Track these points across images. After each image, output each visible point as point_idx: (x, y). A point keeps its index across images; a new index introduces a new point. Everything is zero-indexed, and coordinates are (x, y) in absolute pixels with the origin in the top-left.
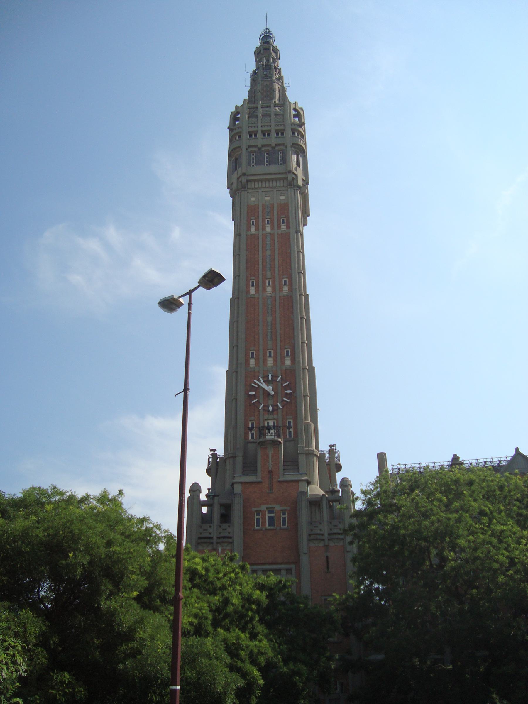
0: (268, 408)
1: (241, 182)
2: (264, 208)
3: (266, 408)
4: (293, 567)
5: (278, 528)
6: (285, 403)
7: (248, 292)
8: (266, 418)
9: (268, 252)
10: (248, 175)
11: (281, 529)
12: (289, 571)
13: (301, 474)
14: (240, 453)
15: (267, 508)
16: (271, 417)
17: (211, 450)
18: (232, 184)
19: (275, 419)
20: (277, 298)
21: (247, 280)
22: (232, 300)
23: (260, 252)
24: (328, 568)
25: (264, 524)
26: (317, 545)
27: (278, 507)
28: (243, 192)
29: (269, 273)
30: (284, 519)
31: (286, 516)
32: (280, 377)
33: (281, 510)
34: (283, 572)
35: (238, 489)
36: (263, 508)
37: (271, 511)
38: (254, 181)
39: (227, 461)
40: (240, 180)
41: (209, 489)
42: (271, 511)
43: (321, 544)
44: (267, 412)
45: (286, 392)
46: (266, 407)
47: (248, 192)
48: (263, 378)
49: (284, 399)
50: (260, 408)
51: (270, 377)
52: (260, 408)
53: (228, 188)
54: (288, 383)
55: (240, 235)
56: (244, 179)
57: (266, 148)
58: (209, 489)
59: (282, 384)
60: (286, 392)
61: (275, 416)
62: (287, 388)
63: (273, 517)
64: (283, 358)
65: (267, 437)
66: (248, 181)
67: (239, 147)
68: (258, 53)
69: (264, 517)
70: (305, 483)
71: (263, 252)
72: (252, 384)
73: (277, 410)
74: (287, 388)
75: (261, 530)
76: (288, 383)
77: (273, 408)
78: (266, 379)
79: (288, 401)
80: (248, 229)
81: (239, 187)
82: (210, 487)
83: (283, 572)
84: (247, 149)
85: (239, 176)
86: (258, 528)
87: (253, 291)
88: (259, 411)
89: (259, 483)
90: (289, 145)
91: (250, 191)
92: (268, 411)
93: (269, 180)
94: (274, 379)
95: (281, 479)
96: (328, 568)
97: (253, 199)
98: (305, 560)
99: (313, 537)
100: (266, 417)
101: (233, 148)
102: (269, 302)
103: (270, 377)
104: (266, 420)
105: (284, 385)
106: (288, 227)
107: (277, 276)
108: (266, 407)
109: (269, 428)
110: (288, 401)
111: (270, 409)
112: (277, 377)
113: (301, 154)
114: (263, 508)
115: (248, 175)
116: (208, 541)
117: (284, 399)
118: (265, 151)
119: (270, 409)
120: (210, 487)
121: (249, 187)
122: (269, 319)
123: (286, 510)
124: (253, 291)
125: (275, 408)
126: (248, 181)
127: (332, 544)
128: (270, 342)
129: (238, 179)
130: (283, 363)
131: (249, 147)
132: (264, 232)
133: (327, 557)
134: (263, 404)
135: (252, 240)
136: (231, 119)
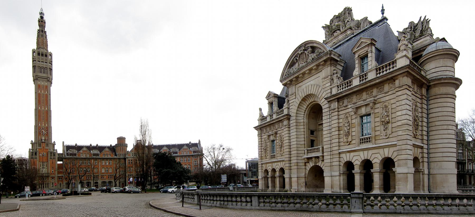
2: (42, 85)
4: (47, 162)
7: (38, 108)
12: (46, 163)
14: (38, 143)
21: (38, 105)
29: (43, 104)
36: (42, 153)
57: (43, 68)
62: (46, 131)
64: (46, 124)
68: (39, 21)
74: (46, 131)
80: (38, 92)
87: (39, 108)
90: (48, 68)
98: (49, 162)
99: (51, 158)
102: (43, 111)
106: (47, 93)
113: (51, 70)
114: (42, 153)
122: (43, 115)
124: (39, 108)
127: (54, 159)
128: (43, 121)
135: (39, 94)
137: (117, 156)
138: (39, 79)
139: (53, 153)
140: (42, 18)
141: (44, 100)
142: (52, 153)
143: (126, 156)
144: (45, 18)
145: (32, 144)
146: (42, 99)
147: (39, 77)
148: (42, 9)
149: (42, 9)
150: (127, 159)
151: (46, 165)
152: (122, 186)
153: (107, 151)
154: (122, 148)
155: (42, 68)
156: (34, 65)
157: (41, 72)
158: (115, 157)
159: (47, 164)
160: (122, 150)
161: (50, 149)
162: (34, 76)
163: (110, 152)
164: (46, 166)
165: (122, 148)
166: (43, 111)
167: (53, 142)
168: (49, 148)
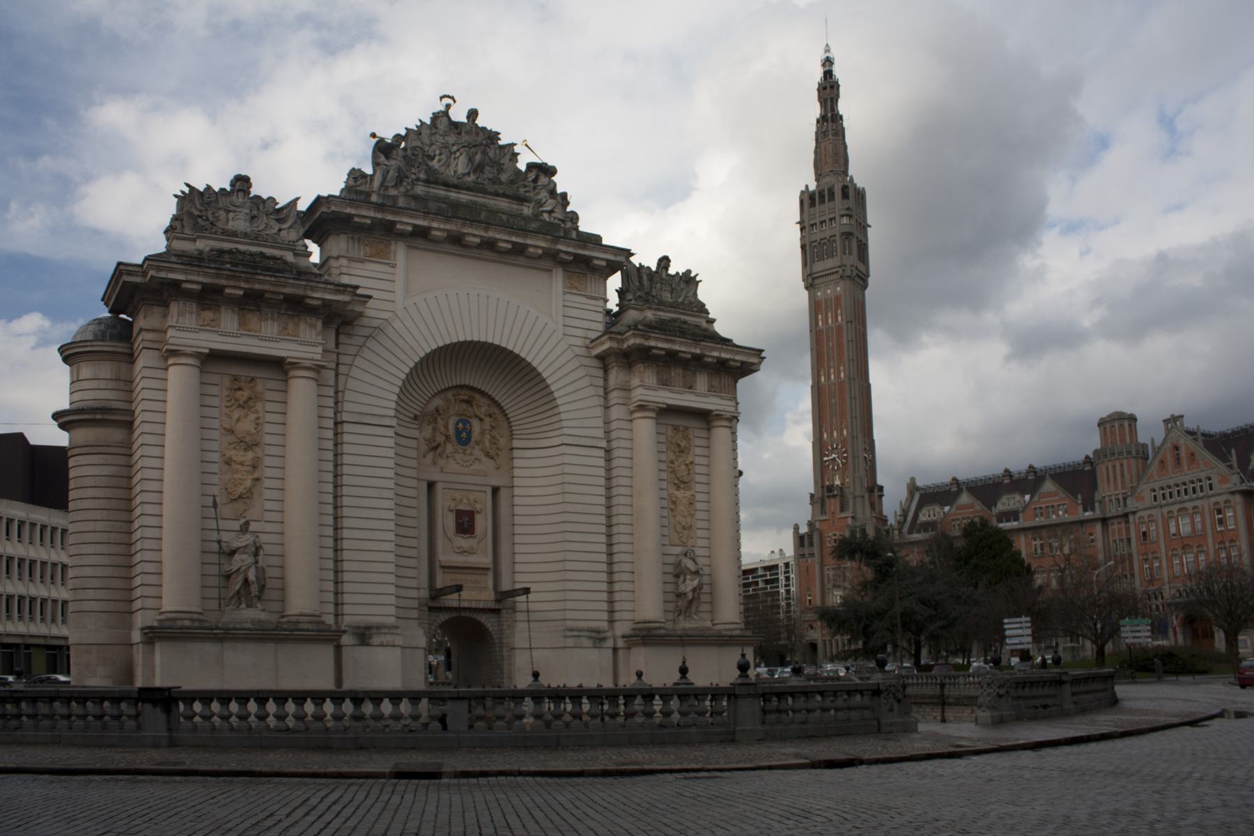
9: (831, 344)
37: (835, 535)
38: (818, 277)
42: (835, 535)
46: (833, 466)
53: (803, 280)
66: (814, 279)
74: (844, 452)
84: (810, 246)
89: (827, 520)
93: (828, 275)
108: (833, 466)
114: (830, 534)
118: (824, 243)
122: (833, 401)
137: (1093, 509)
138: (817, 281)
140: (828, 74)
141: (833, 347)
143: (1125, 505)
144: (838, 72)
146: (828, 345)
148: (827, 50)
149: (827, 50)
150: (1131, 518)
153: (1051, 494)
154: (1111, 469)
155: (823, 241)
157: (821, 258)
158: (1087, 514)
160: (1115, 477)
161: (853, 517)
163: (1062, 495)
165: (1111, 469)
166: (833, 387)
168: (850, 515)
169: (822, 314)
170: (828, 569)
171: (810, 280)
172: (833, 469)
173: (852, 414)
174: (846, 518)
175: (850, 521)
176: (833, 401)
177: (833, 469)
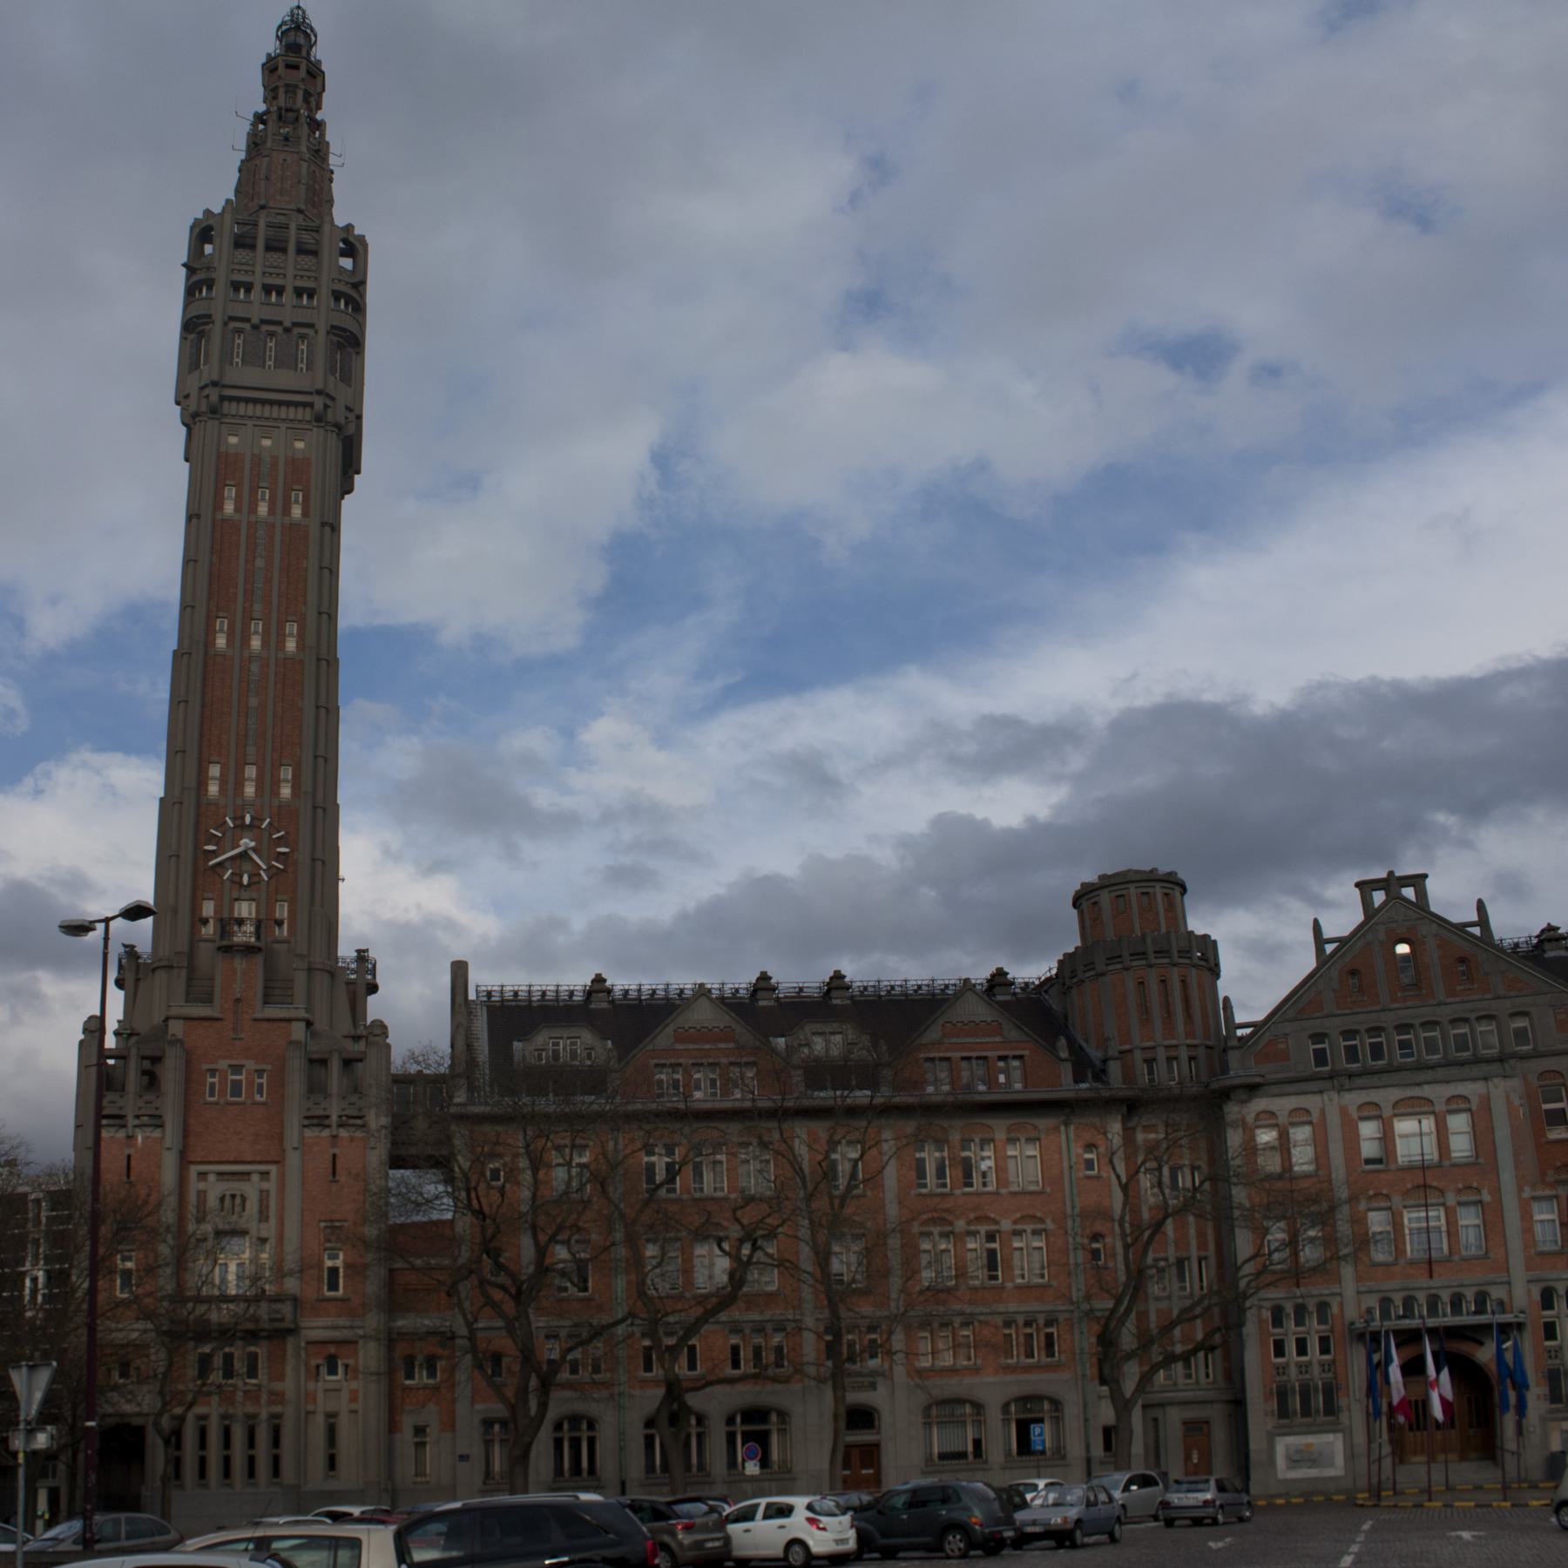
0: (241, 877)
1: (207, 397)
3: (236, 879)
4: (273, 1169)
5: (249, 1102)
6: (275, 871)
8: (236, 896)
9: (260, 563)
10: (224, 386)
11: (255, 1103)
12: (265, 1175)
13: (297, 1008)
15: (230, 1066)
16: (244, 895)
17: (125, 946)
18: (187, 396)
19: (254, 900)
20: (272, 663)
22: (177, 655)
23: (242, 561)
24: (334, 1174)
25: (222, 1092)
26: (317, 1134)
27: (251, 1065)
28: (210, 423)
30: (260, 1085)
31: (264, 1081)
32: (268, 820)
33: (256, 1071)
34: (255, 1178)
35: (176, 1028)
37: (237, 1069)
38: (239, 400)
39: (158, 973)
40: (206, 392)
41: (119, 1021)
43: (326, 1133)
44: (237, 886)
45: (280, 850)
47: (222, 423)
48: (234, 819)
49: (274, 863)
50: (225, 878)
51: (248, 820)
52: (225, 878)
54: (282, 833)
55: (198, 516)
56: (214, 395)
58: (119, 1021)
59: (271, 835)
60: (280, 850)
61: (254, 895)
63: (241, 1081)
65: (235, 939)
66: (222, 398)
67: (209, 316)
69: (223, 1081)
70: (302, 1025)
71: (247, 561)
72: (212, 831)
73: (259, 882)
75: (217, 1103)
76: (282, 833)
77: (249, 878)
78: (238, 822)
79: (281, 867)
80: (218, 505)
81: (204, 408)
82: (121, 1018)
83: (255, 1178)
84: (226, 324)
85: (202, 384)
86: (212, 1099)
88: (222, 883)
91: (224, 420)
92: (241, 884)
94: (256, 823)
95: (258, 1016)
96: (334, 1174)
97: (233, 440)
98: (293, 1160)
100: (235, 895)
101: (193, 315)
102: (255, 668)
103: (248, 820)
104: (237, 900)
105: (274, 836)
107: (274, 616)
109: (240, 922)
110: (281, 867)
111: (245, 880)
112: (263, 820)
115: (224, 386)
116: (117, 1122)
117: (274, 863)
119: (245, 880)
120: (121, 1018)
121: (225, 411)
122: (253, 702)
123: (264, 1071)
125: (256, 879)
126: (222, 398)
127: (343, 1133)
129: (202, 388)
130: (276, 793)
131: (232, 319)
132: (253, 518)
133: (334, 1156)
134: (230, 871)
136: (193, 238)
138: (228, 408)
139: (335, 1065)
142: (323, 1062)
145: (129, 982)
147: (231, 399)
151: (264, 1196)
152: (1188, 1458)
156: (199, 309)
159: (271, 1186)
161: (309, 1024)
162: (187, 396)
164: (263, 1216)
166: (255, 668)
167: (346, 950)
168: (302, 1014)
169: (239, 486)
170: (202, 1176)
171: (214, 398)
172: (236, 880)
173: (316, 747)
174: (289, 1020)
175: (298, 1032)
176: (253, 702)
177: (236, 880)
